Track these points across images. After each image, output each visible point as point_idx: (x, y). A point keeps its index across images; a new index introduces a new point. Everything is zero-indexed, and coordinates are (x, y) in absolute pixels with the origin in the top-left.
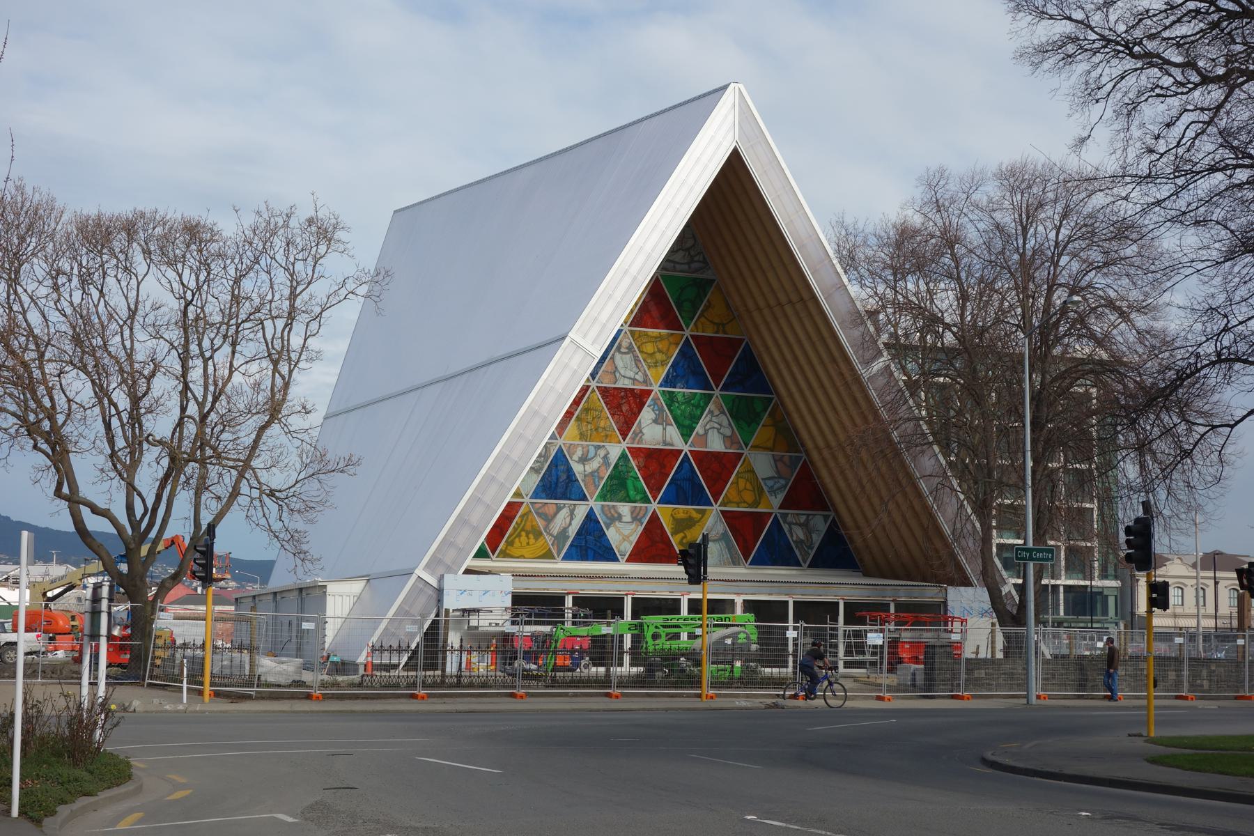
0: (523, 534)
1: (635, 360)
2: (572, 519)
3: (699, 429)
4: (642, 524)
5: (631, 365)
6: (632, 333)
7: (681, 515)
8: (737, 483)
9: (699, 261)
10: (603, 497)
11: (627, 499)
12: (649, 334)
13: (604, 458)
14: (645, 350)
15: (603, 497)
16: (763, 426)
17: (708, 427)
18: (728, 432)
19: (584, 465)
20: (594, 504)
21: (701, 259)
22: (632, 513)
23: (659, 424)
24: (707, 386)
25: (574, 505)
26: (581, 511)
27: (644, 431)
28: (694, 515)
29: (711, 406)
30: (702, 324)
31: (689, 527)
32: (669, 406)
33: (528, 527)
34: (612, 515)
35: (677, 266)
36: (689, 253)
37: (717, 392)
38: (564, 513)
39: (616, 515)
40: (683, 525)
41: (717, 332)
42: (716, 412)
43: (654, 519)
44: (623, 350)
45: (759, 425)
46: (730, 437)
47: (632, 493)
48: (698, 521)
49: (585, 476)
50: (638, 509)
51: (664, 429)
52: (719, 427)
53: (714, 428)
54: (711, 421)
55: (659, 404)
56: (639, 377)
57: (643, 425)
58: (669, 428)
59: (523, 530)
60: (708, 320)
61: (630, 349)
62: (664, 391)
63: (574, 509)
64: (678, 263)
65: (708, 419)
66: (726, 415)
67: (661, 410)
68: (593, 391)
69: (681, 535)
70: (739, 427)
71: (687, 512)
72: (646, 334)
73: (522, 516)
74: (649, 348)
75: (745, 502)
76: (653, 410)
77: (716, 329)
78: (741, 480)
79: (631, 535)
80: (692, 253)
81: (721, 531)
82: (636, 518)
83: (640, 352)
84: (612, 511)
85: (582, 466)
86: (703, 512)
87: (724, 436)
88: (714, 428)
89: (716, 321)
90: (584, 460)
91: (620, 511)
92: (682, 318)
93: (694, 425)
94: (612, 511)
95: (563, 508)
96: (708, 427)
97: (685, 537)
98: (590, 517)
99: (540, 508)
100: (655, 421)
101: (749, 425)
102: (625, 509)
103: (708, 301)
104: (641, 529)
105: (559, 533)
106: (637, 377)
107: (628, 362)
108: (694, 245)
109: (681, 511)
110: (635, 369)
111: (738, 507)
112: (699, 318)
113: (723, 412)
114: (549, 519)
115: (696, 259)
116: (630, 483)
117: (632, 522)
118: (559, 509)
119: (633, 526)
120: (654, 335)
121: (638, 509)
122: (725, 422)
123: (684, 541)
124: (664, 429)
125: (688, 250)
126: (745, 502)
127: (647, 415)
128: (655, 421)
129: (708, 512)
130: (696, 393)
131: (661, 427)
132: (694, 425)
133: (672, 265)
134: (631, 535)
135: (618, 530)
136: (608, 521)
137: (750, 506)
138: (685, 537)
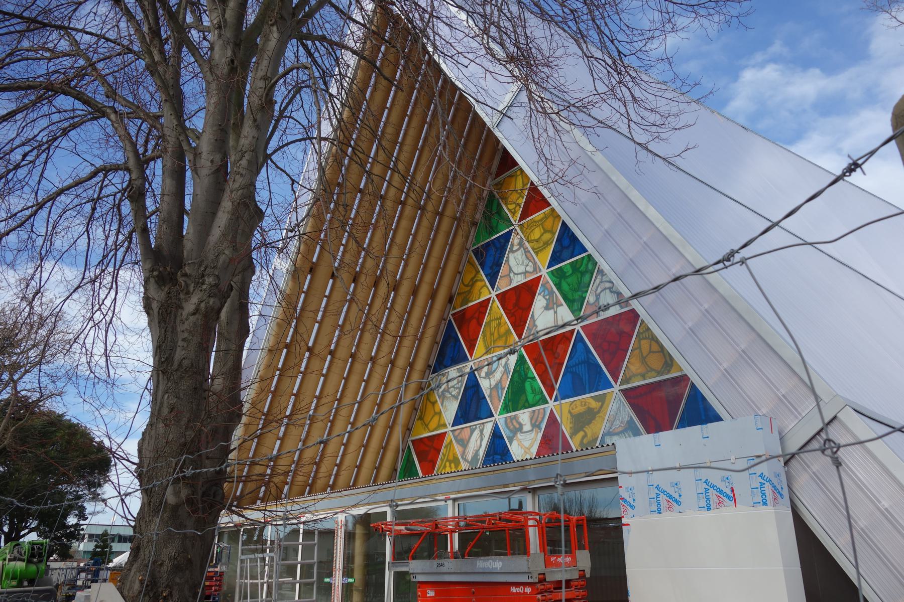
0: (448, 464)
1: (525, 252)
2: (482, 440)
4: (540, 429)
5: (522, 259)
7: (580, 409)
8: (640, 348)
10: (506, 409)
11: (527, 404)
13: (505, 365)
15: (506, 409)
19: (489, 378)
20: (500, 418)
22: (531, 419)
23: (550, 309)
25: (483, 424)
26: (488, 429)
27: (537, 323)
28: (594, 404)
31: (589, 423)
32: (559, 286)
33: (451, 458)
34: (514, 427)
38: (476, 434)
39: (517, 426)
40: (582, 420)
43: (553, 421)
44: (515, 248)
47: (530, 397)
48: (599, 412)
49: (491, 389)
50: (537, 412)
51: (556, 312)
53: (605, 289)
54: (601, 282)
55: (548, 287)
56: (530, 269)
57: (536, 317)
58: (560, 309)
59: (448, 460)
61: (521, 244)
63: (483, 429)
65: (598, 281)
67: (551, 293)
68: (494, 301)
69: (581, 434)
71: (583, 403)
72: (533, 221)
73: (446, 447)
75: (652, 370)
76: (544, 297)
78: (643, 342)
79: (532, 445)
81: (626, 419)
82: (535, 425)
84: (515, 423)
85: (488, 380)
86: (602, 399)
88: (605, 289)
90: (489, 375)
91: (520, 420)
94: (515, 423)
95: (476, 428)
97: (585, 436)
98: (496, 435)
99: (459, 434)
100: (547, 308)
102: (524, 416)
104: (540, 435)
105: (472, 458)
106: (529, 269)
107: (520, 259)
109: (578, 403)
110: (526, 262)
111: (644, 379)
114: (464, 444)
116: (528, 385)
117: (532, 430)
118: (472, 432)
119: (533, 434)
121: (537, 412)
123: (585, 441)
124: (556, 312)
126: (652, 370)
127: (539, 302)
128: (547, 308)
129: (608, 397)
130: (583, 258)
131: (552, 312)
134: (532, 445)
135: (520, 444)
136: (511, 435)
137: (660, 373)
138: (585, 436)
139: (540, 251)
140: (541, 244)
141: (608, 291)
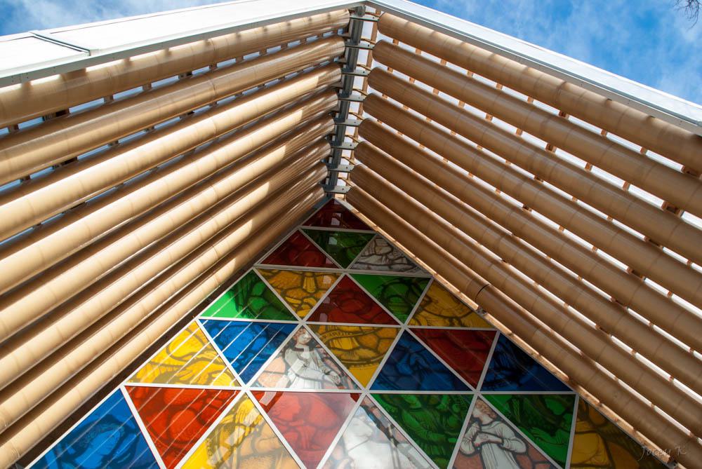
3: (462, 444)
6: (312, 327)
9: (404, 264)
12: (344, 328)
14: (337, 346)
16: (576, 433)
17: (478, 441)
18: (520, 447)
21: (405, 261)
24: (458, 385)
29: (474, 411)
30: (425, 318)
35: (371, 266)
36: (386, 258)
37: (477, 392)
41: (452, 325)
42: (486, 420)
45: (569, 432)
46: (526, 453)
52: (500, 440)
53: (489, 442)
54: (480, 432)
60: (435, 315)
62: (381, 395)
64: (373, 265)
66: (504, 422)
70: (535, 438)
72: (339, 329)
74: (347, 344)
77: (447, 321)
80: (391, 257)
83: (329, 348)
87: (515, 454)
88: (489, 442)
89: (445, 313)
92: (392, 312)
93: (451, 440)
96: (478, 441)
101: (552, 432)
103: (426, 296)
108: (392, 251)
112: (417, 313)
113: (498, 418)
115: (397, 261)
120: (351, 329)
122: (507, 433)
125: (386, 254)
130: (441, 396)
132: (451, 440)
133: (366, 266)
139: (355, 365)
140: (357, 358)
141: (494, 446)
